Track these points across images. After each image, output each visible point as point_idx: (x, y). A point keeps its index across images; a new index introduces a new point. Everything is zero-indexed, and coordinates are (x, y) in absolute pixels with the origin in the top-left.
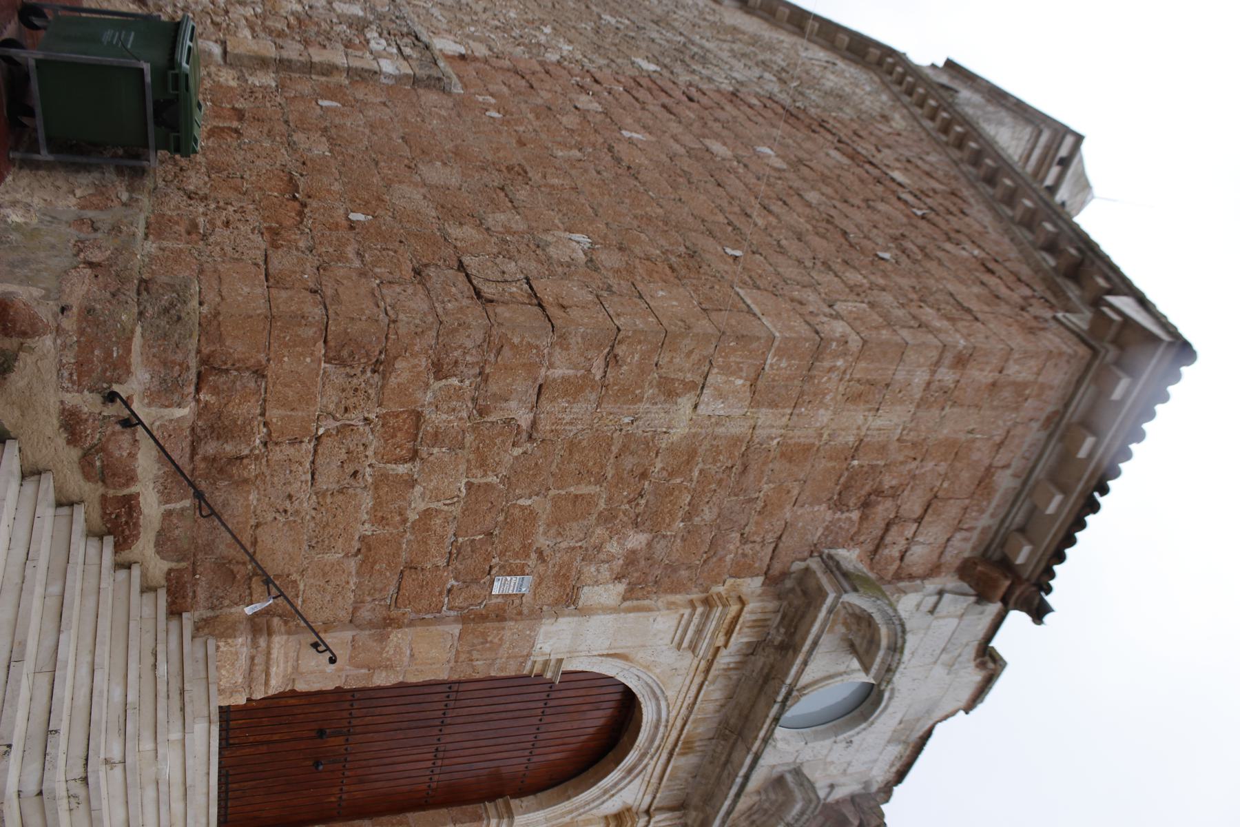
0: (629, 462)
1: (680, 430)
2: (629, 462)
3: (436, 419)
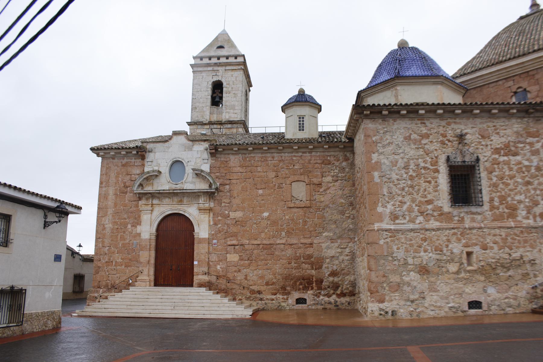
0: (115, 231)
1: (111, 225)
2: (115, 231)
3: (107, 260)
